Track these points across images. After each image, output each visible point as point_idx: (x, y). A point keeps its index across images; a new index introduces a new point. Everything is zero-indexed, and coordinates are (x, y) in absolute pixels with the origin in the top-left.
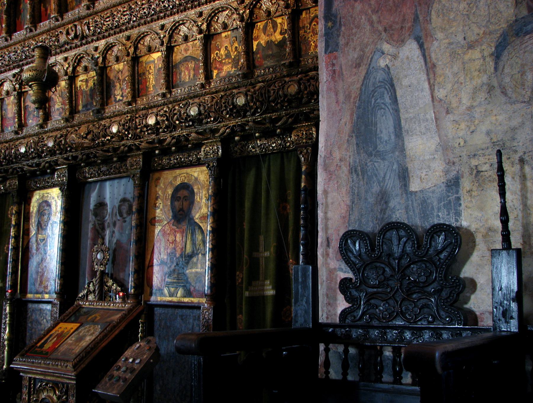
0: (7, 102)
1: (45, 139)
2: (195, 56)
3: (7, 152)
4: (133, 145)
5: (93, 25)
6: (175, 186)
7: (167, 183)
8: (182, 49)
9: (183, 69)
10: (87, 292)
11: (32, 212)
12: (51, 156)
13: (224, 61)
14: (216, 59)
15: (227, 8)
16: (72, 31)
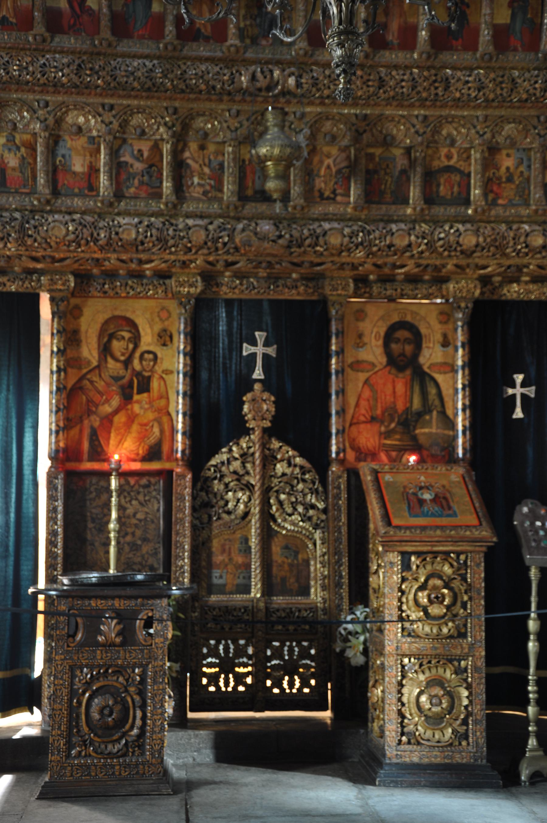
0: (69, 143)
1: (181, 226)
2: (462, 168)
3: (86, 233)
4: (348, 264)
5: (310, 81)
6: (389, 323)
7: (376, 318)
8: (443, 154)
9: (442, 181)
10: (228, 459)
11: (87, 332)
12: (185, 253)
13: (503, 185)
14: (491, 179)
15: (520, 123)
16: (265, 77)
